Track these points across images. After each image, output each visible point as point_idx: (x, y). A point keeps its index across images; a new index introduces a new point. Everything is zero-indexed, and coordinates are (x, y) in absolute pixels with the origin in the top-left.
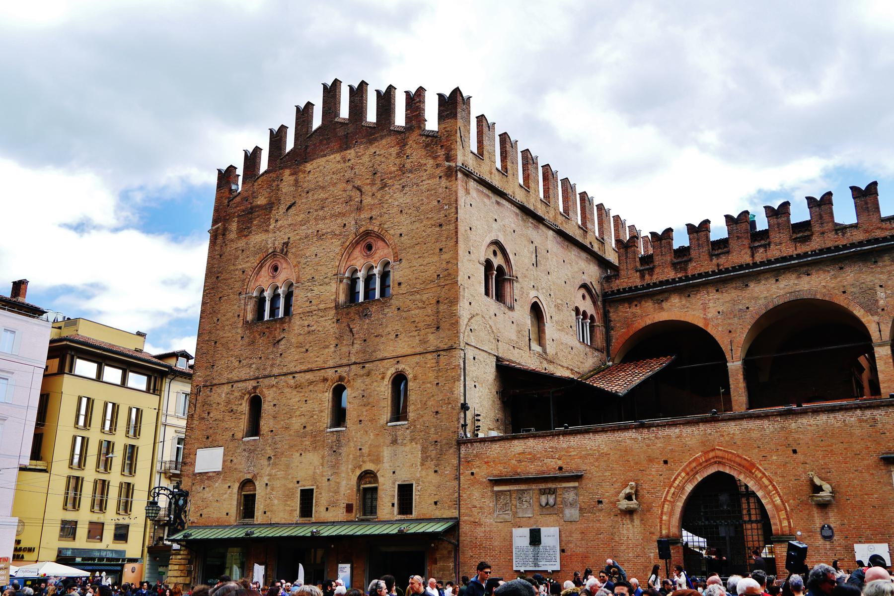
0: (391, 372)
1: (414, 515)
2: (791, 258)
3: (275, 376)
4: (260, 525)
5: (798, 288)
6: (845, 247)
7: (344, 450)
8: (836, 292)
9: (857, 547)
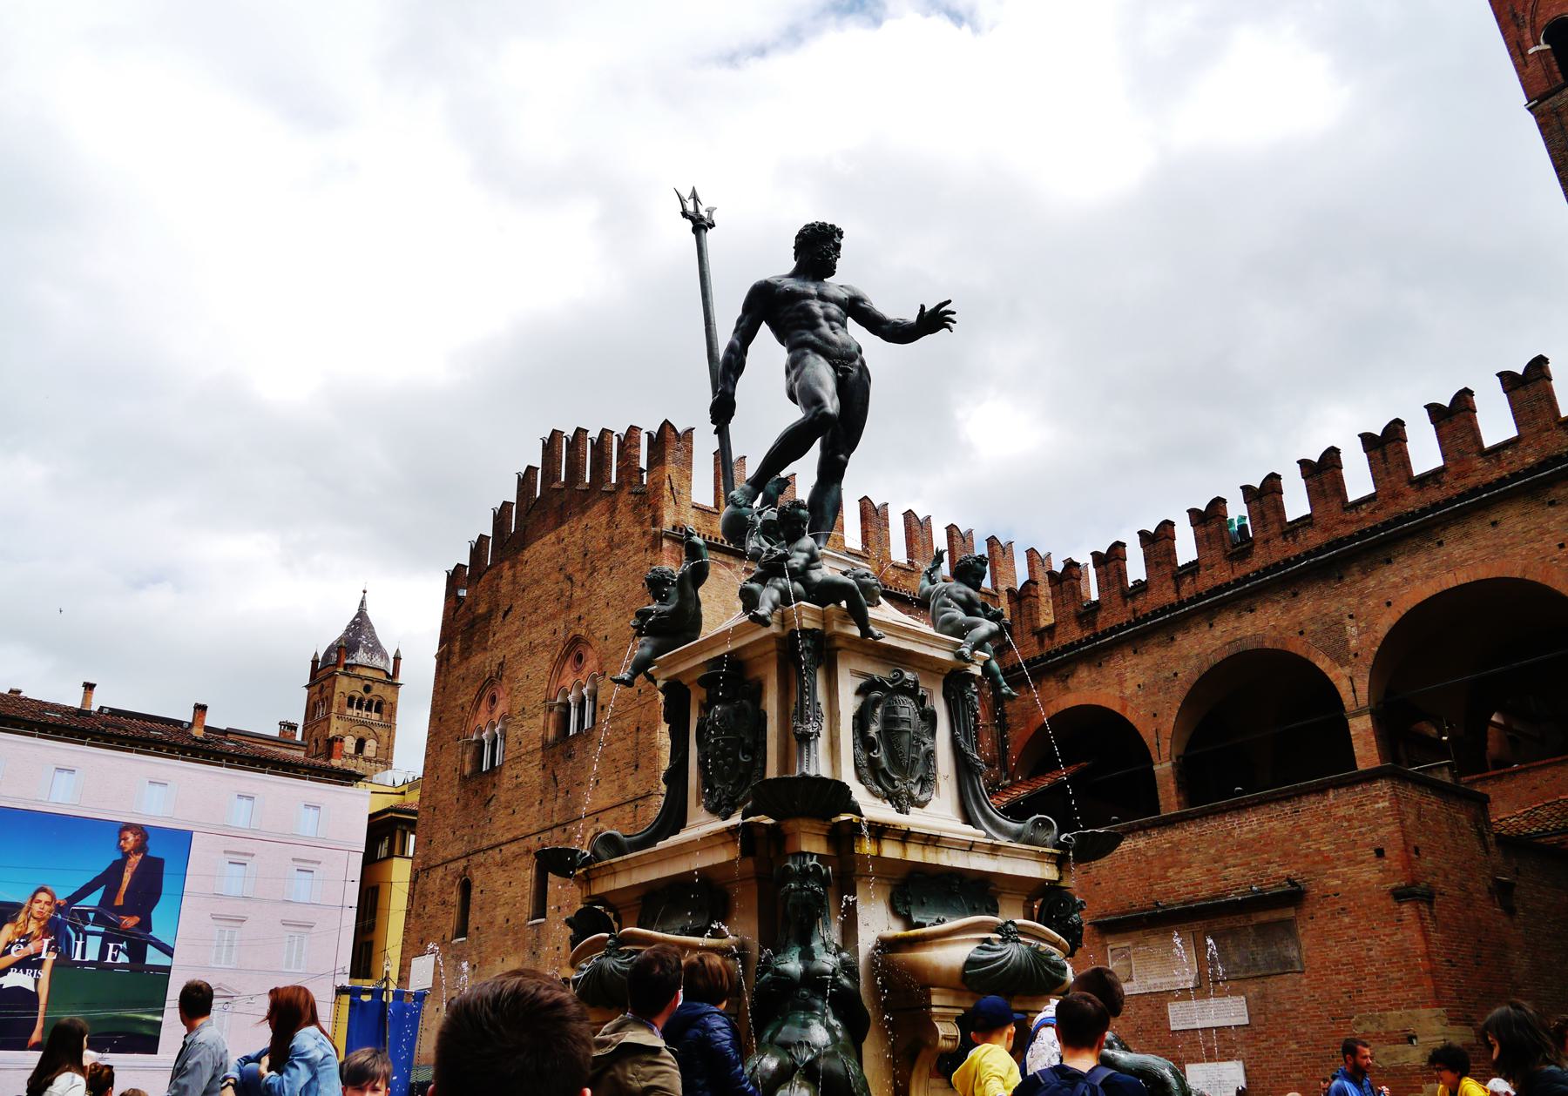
2: (1228, 586)
3: (484, 851)
5: (1239, 634)
6: (1298, 559)
8: (1290, 633)
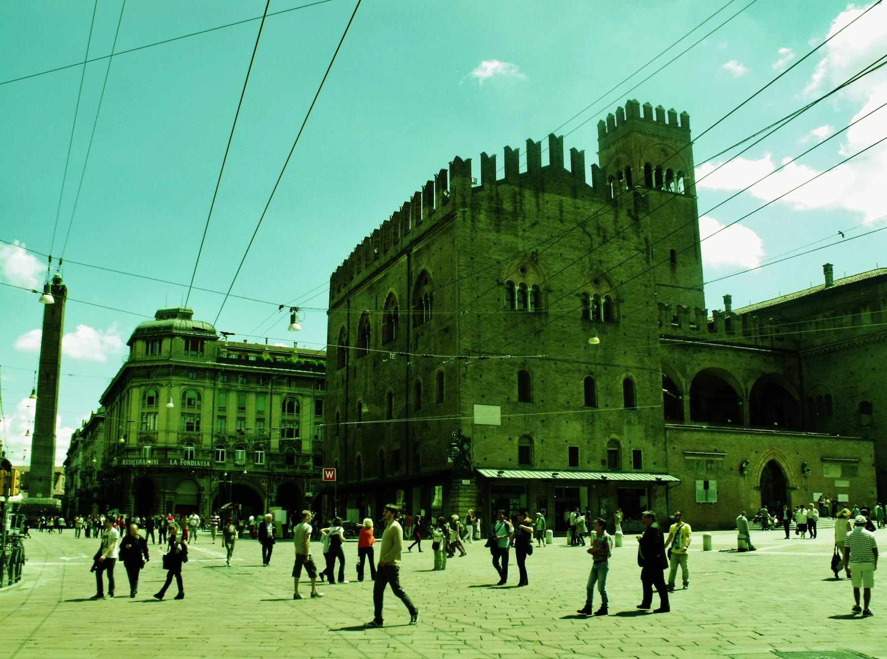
0: (624, 376)
1: (643, 468)
7: (597, 423)
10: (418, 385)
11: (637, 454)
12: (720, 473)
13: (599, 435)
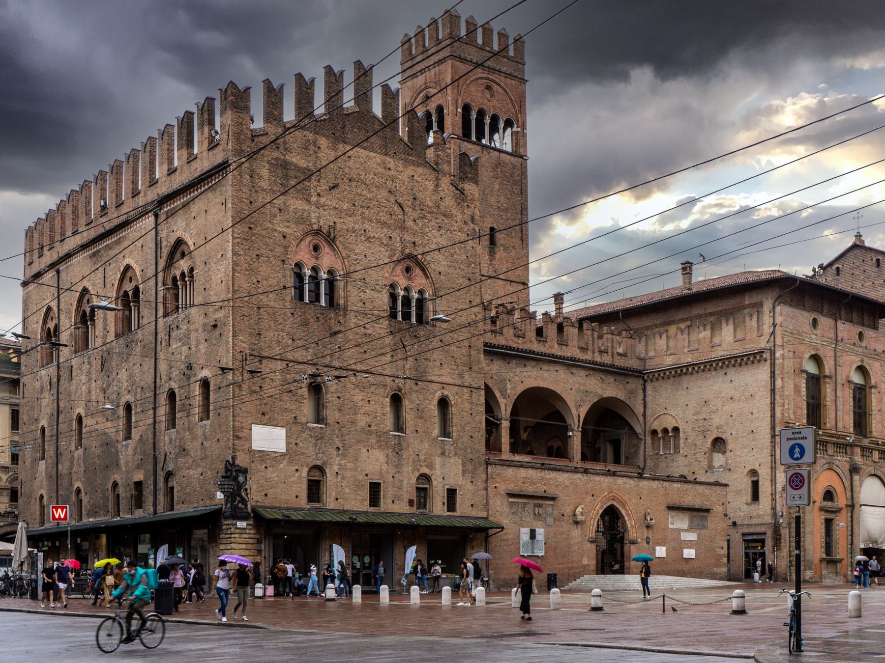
0: (438, 394)
4: (332, 511)
7: (405, 453)
9: (657, 548)
10: (172, 395)
11: (452, 494)
12: (550, 520)
13: (407, 469)
